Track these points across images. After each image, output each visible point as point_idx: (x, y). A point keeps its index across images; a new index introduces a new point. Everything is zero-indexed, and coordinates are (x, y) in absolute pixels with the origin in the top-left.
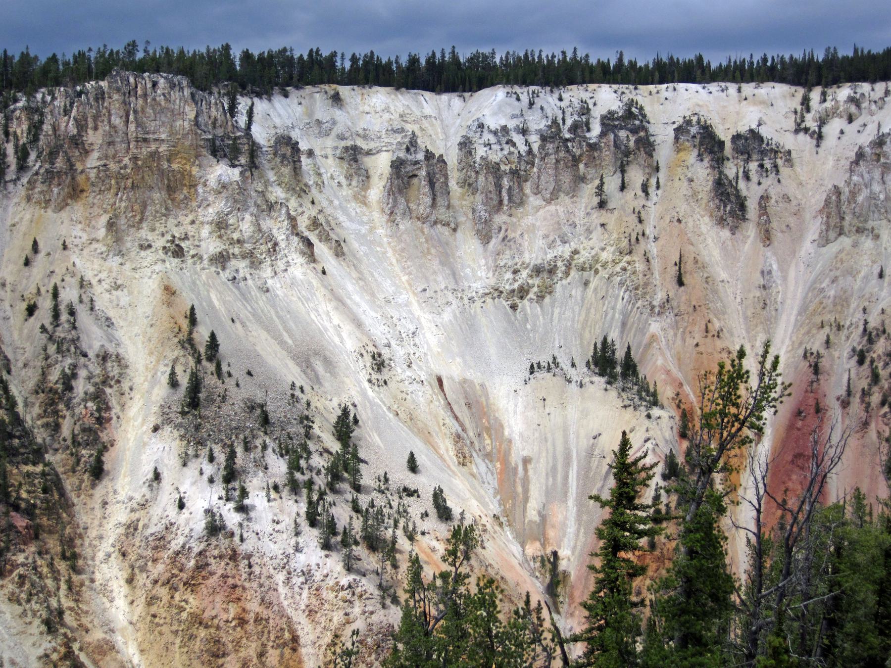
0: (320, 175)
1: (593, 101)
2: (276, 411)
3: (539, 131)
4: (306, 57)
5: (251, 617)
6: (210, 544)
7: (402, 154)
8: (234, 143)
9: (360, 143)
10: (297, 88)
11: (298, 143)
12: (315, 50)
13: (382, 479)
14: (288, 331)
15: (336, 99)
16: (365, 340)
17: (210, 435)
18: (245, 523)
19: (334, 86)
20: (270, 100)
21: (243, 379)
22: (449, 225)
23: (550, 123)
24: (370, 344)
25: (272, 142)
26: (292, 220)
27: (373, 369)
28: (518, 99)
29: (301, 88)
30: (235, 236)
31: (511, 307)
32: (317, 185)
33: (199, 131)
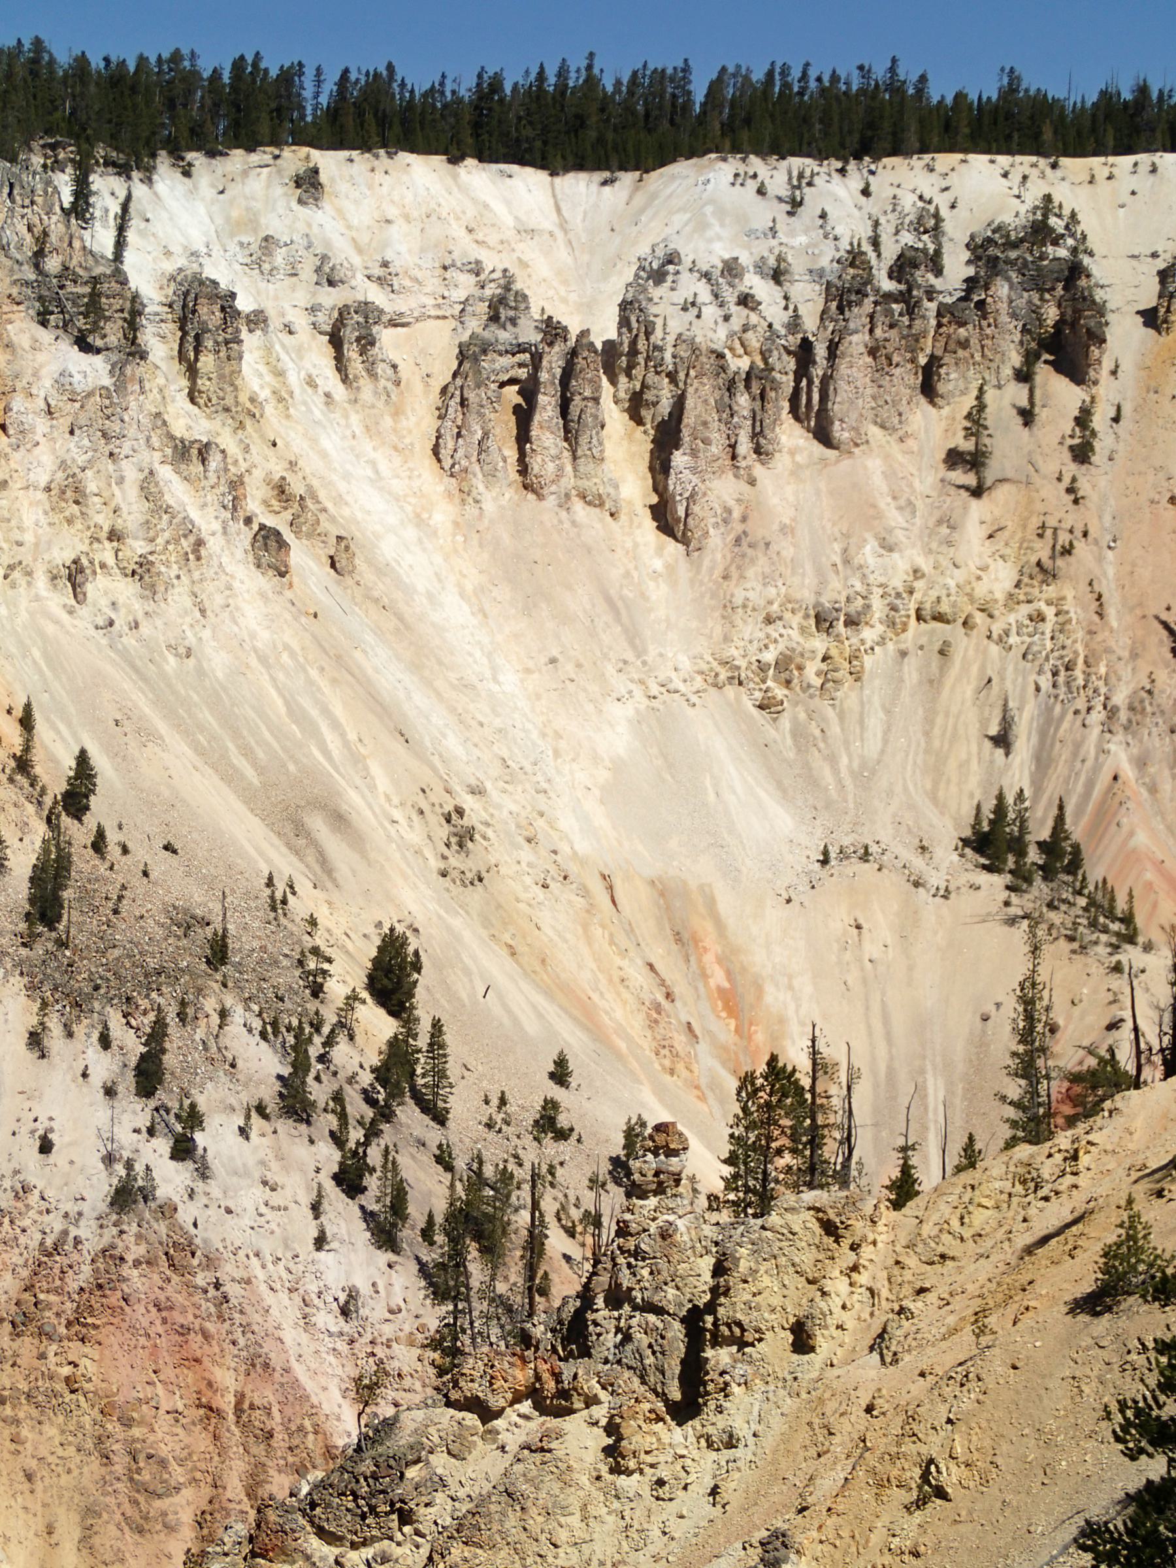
0: (280, 374)
1: (948, 197)
2: (248, 935)
3: (817, 274)
4: (226, 78)
5: (227, 1403)
6: (122, 1232)
7: (474, 325)
8: (95, 296)
9: (377, 296)
10: (212, 154)
11: (233, 295)
12: (250, 59)
13: (495, 1102)
14: (247, 752)
15: (309, 184)
16: (426, 777)
17: (97, 988)
18: (200, 1186)
19: (306, 149)
20: (148, 181)
21: (161, 864)
22: (601, 505)
23: (842, 253)
24: (439, 789)
25: (171, 292)
26: (236, 484)
27: (448, 845)
28: (761, 191)
29: (222, 154)
30: (104, 521)
31: (761, 707)
32: (281, 400)
33: (9, 263)
